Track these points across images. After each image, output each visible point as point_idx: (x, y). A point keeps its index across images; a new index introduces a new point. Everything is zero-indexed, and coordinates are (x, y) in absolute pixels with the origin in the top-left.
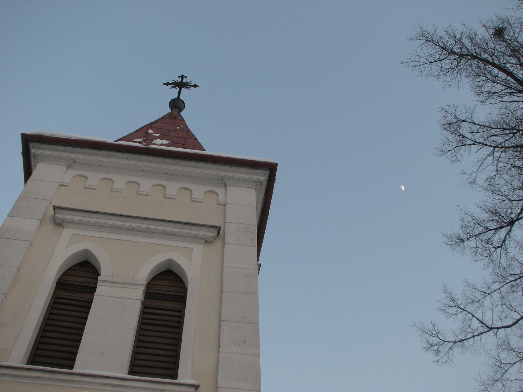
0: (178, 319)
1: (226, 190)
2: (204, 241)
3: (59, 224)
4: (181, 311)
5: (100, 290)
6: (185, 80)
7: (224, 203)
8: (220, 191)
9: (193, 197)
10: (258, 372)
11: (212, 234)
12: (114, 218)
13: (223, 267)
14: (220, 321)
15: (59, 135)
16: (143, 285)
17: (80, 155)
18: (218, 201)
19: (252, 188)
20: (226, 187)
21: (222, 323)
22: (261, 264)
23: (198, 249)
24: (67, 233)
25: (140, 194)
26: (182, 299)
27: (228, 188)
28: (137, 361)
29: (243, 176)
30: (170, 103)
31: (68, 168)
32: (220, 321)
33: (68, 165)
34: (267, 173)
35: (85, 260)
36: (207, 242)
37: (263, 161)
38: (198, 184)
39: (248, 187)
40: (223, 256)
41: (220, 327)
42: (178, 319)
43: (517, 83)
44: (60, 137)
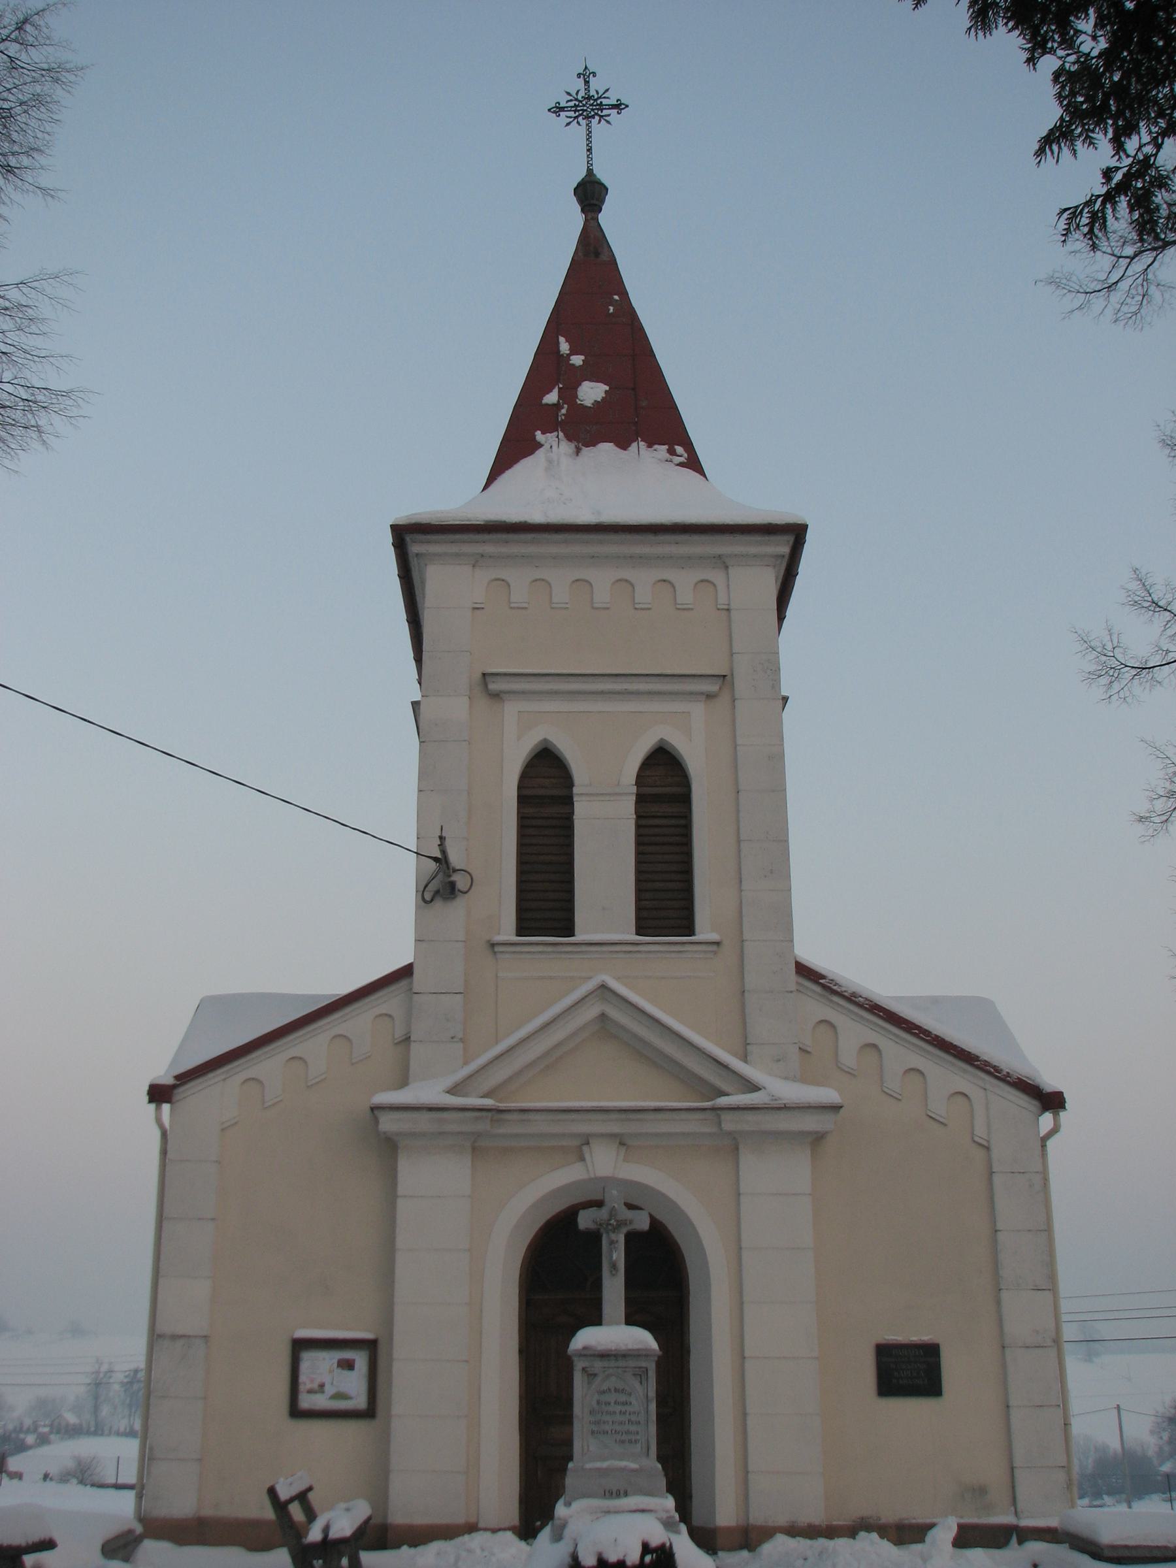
0: (683, 822)
1: (728, 574)
2: (704, 696)
3: (496, 696)
4: (686, 817)
5: (581, 809)
6: (596, 85)
7: (726, 607)
8: (717, 577)
9: (679, 601)
10: (790, 915)
11: (712, 687)
12: (571, 679)
13: (735, 746)
14: (739, 841)
15: (450, 519)
16: (633, 793)
17: (490, 546)
18: (717, 605)
19: (768, 566)
20: (727, 567)
21: (742, 844)
22: (788, 698)
23: (698, 710)
24: (511, 709)
25: (597, 608)
26: (685, 799)
27: (731, 570)
28: (644, 902)
29: (753, 550)
30: (575, 189)
31: (474, 566)
32: (739, 841)
33: (473, 562)
34: (791, 539)
35: (544, 747)
36: (710, 696)
37: (784, 523)
38: (683, 568)
39: (762, 565)
40: (734, 721)
41: (739, 851)
42: (683, 822)
43: (885, 1016)
44: (451, 523)
